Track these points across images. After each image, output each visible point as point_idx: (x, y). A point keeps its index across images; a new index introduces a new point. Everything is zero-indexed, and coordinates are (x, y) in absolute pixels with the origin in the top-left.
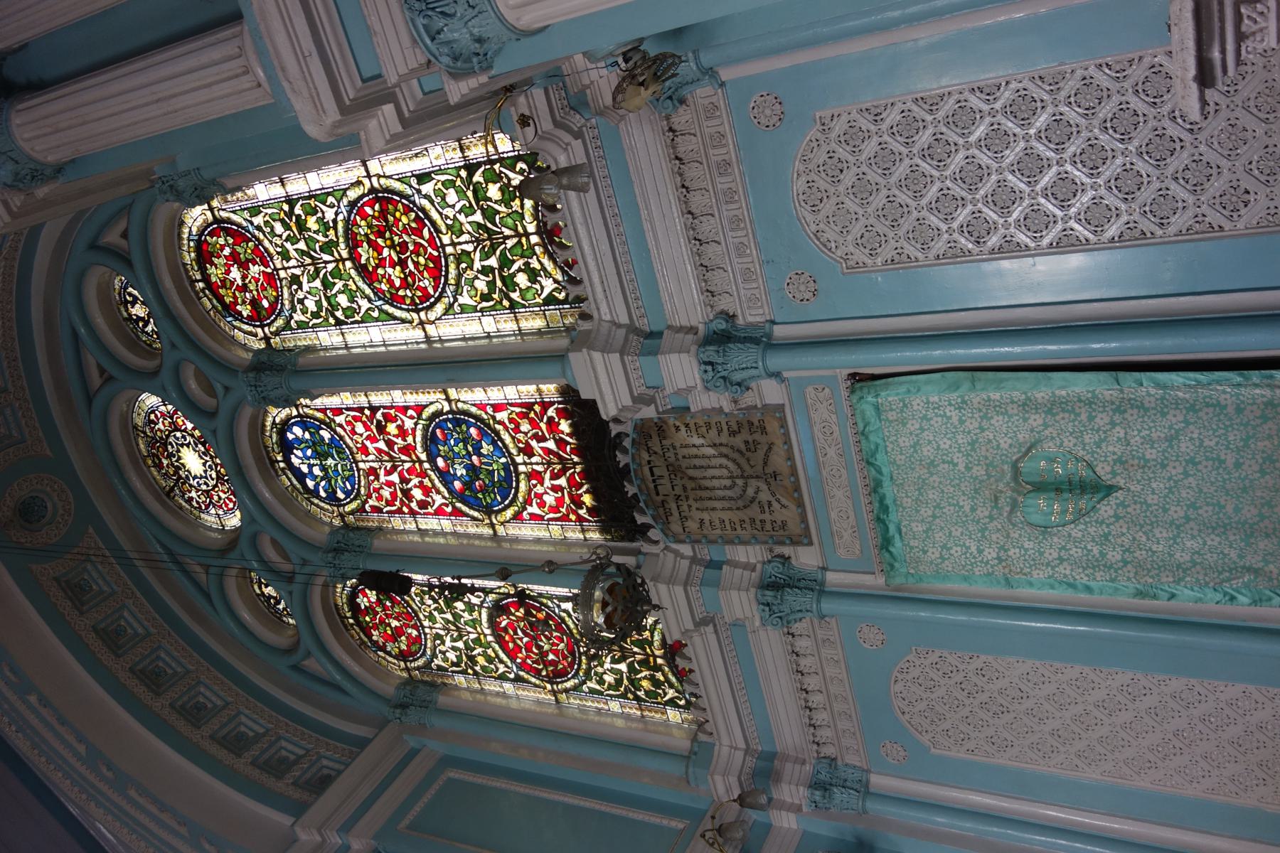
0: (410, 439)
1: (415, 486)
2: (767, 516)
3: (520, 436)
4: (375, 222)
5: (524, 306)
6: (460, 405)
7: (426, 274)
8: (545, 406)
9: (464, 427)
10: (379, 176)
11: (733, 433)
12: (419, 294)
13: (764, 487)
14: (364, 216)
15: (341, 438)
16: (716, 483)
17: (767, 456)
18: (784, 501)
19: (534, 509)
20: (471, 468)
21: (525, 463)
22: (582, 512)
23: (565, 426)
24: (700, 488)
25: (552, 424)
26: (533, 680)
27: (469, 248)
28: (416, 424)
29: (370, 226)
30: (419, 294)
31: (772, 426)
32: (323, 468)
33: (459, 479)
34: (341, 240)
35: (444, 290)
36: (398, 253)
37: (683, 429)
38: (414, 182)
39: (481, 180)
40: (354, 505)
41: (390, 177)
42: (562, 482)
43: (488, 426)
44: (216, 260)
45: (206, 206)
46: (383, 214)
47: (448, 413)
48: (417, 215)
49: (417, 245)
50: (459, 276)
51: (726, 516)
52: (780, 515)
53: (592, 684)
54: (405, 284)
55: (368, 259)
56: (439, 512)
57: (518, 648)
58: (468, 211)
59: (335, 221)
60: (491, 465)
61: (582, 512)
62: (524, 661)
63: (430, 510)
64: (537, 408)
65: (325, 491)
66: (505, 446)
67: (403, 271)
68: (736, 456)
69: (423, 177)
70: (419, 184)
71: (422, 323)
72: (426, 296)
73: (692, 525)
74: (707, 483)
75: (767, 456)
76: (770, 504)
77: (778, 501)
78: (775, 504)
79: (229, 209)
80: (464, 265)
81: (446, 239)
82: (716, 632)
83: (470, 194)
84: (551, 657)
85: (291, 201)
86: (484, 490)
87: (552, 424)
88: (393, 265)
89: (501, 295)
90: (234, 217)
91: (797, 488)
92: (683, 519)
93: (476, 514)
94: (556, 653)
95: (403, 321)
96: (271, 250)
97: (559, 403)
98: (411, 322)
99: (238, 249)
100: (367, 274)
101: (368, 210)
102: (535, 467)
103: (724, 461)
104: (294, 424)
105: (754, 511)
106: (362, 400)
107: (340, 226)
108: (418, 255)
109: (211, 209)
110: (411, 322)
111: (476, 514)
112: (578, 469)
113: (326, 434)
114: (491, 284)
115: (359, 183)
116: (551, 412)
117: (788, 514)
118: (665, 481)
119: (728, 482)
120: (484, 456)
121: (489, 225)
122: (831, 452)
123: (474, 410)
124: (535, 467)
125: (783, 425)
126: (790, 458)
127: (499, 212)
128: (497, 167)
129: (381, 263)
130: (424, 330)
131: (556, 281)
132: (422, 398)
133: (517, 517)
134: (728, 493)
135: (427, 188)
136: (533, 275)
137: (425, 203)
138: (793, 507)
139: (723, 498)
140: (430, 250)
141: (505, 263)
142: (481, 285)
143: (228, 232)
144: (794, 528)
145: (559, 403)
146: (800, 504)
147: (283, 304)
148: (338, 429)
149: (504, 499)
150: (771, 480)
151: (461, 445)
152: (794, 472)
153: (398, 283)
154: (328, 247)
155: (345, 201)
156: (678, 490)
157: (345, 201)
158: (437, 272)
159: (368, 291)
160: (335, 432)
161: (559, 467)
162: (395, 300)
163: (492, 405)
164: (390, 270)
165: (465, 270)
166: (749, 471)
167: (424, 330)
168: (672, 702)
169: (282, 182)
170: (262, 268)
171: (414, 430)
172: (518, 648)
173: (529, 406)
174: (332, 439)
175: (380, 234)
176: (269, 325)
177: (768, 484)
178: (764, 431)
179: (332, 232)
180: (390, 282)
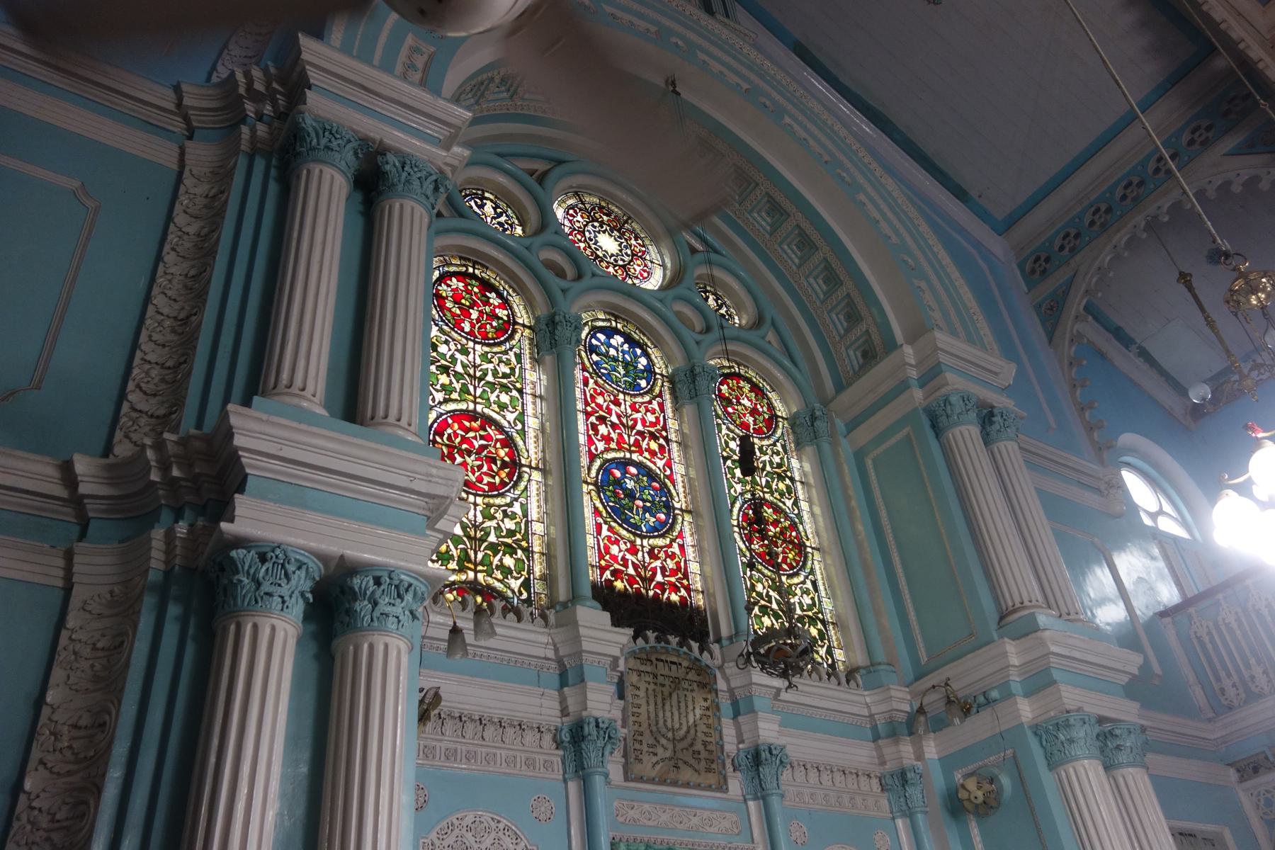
2: (645, 748)
8: (688, 589)
11: (705, 744)
13: (668, 754)
16: (668, 714)
17: (691, 766)
18: (658, 767)
19: (605, 532)
20: (631, 495)
22: (607, 574)
23: (674, 598)
24: (664, 699)
31: (712, 779)
32: (615, 359)
37: (706, 704)
40: (587, 364)
42: (631, 571)
46: (791, 542)
51: (643, 710)
52: (648, 760)
56: (591, 442)
57: (467, 430)
61: (607, 574)
63: (591, 432)
66: (654, 537)
68: (689, 740)
69: (814, 583)
73: (634, 678)
74: (667, 707)
75: (691, 766)
76: (655, 754)
77: (657, 763)
78: (654, 759)
82: (546, 658)
84: (459, 460)
86: (615, 494)
91: (663, 782)
92: (640, 673)
103: (685, 728)
105: (647, 739)
116: (683, 592)
117: (647, 766)
118: (666, 672)
119: (669, 724)
122: (695, 821)
125: (709, 788)
126: (687, 785)
133: (597, 512)
134: (661, 722)
135: (809, 585)
137: (801, 578)
138: (653, 774)
139: (657, 715)
143: (771, 418)
144: (637, 769)
146: (651, 781)
150: (672, 763)
152: (674, 783)
154: (768, 485)
156: (661, 679)
166: (680, 746)
172: (462, 427)
174: (638, 387)
175: (782, 532)
177: (670, 759)
178: (708, 770)
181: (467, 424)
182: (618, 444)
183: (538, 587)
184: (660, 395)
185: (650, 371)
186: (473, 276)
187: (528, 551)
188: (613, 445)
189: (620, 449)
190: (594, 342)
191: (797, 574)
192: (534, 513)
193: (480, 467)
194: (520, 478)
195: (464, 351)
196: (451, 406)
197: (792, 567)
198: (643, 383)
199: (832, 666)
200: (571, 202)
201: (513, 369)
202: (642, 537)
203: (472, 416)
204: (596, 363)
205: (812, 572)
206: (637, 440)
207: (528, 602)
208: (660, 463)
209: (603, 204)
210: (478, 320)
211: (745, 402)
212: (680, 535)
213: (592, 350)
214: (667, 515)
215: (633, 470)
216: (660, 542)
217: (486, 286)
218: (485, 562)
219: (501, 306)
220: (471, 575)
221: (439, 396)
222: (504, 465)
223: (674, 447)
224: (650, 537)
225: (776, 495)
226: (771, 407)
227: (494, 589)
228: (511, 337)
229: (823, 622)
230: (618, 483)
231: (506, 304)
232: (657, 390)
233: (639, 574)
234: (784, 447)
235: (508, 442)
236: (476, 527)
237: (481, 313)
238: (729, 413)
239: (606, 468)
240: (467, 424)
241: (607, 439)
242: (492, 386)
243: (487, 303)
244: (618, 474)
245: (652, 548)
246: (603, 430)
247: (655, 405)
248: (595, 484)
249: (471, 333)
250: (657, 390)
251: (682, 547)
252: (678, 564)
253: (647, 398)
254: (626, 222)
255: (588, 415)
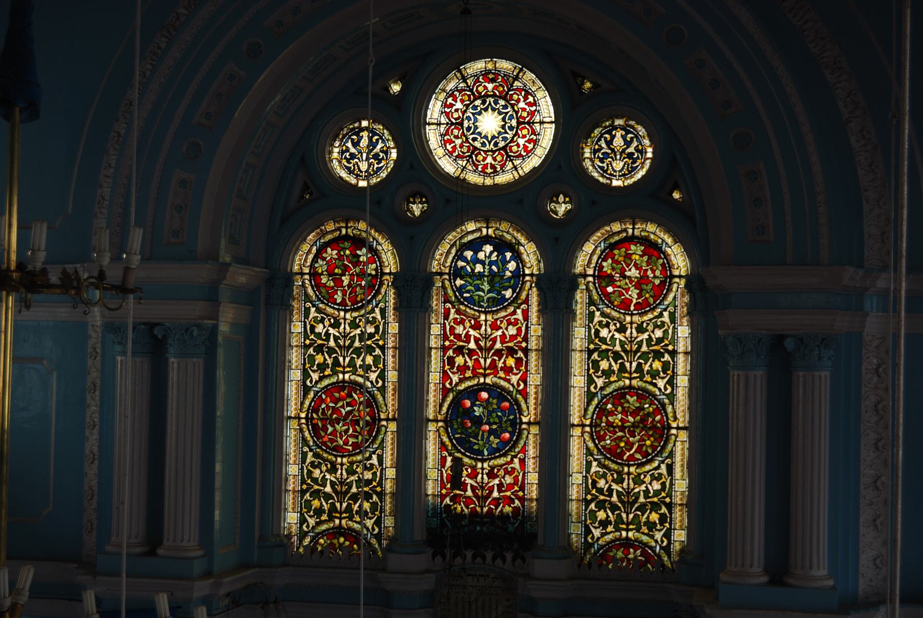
0: (502, 374)
1: (466, 362)
3: (502, 472)
4: (650, 419)
5: (586, 510)
6: (525, 432)
7: (614, 443)
8: (522, 500)
9: (510, 429)
10: (677, 437)
12: (602, 433)
14: (656, 412)
15: (505, 308)
20: (478, 421)
21: (483, 469)
22: (447, 500)
25: (510, 501)
26: (307, 403)
27: (625, 485)
28: (513, 385)
29: (649, 414)
30: (602, 433)
32: (481, 276)
33: (472, 407)
34: (644, 385)
35: (602, 454)
36: (629, 427)
38: (668, 461)
39: (662, 511)
41: (674, 445)
43: (510, 450)
44: (645, 258)
45: (683, 274)
46: (654, 427)
47: (521, 419)
48: (650, 454)
49: (632, 445)
50: (609, 469)
53: (310, 457)
54: (609, 424)
55: (628, 402)
56: (445, 376)
57: (336, 401)
58: (647, 492)
59: (655, 385)
60: (482, 440)
61: (447, 500)
62: (323, 401)
63: (447, 367)
64: (521, 494)
65: (462, 267)
66: (496, 458)
67: (617, 426)
69: (670, 469)
70: (667, 464)
71: (583, 426)
72: (602, 438)
79: (677, 295)
80: (615, 476)
81: (632, 469)
83: (655, 499)
84: (330, 429)
85: (673, 353)
86: (463, 424)
87: (510, 501)
88: (622, 420)
89: (595, 497)
90: (671, 296)
93: (445, 409)
94: (334, 433)
95: (586, 410)
96: (646, 318)
97: (524, 511)
98: (584, 416)
99: (650, 286)
100: (619, 396)
101: (658, 418)
102: (480, 476)
104: (518, 265)
106: (533, 344)
107: (650, 387)
108: (626, 443)
109: (680, 277)
110: (584, 416)
111: (445, 409)
112: (478, 509)
113: (508, 294)
114: (600, 491)
115: (675, 419)
120: (489, 437)
121: (636, 505)
123: (522, 442)
124: (480, 476)
127: (643, 515)
128: (667, 525)
129: (625, 412)
130: (578, 425)
131: (598, 539)
132: (532, 401)
133: (443, 446)
136: (604, 524)
137: (656, 464)
140: (628, 454)
141: (614, 508)
142: (602, 483)
143: (663, 283)
145: (524, 511)
147: (608, 307)
148: (512, 309)
149: (456, 439)
151: (497, 420)
153: (610, 418)
155: (666, 401)
157: (666, 401)
158: (614, 453)
159: (608, 390)
160: (509, 305)
161: (480, 494)
162: (601, 411)
163: (524, 459)
164: (620, 416)
165: (612, 475)
167: (578, 425)
168: (303, 521)
169: (686, 353)
170: (634, 301)
171: (508, 381)
172: (336, 401)
173: (522, 488)
174: (504, 299)
175: (643, 420)
176: (594, 283)
179: (649, 379)
180: (611, 413)
181: (337, 395)
182: (474, 371)
183: (389, 522)
184: (526, 301)
185: (518, 274)
186: (347, 237)
187: (381, 495)
188: (469, 374)
189: (475, 375)
190: (461, 264)
191: (652, 460)
192: (388, 460)
193: (347, 431)
194: (378, 432)
195: (336, 325)
196: (326, 382)
197: (645, 454)
198: (508, 294)
199: (667, 549)
200: (451, 86)
201: (377, 328)
202: (483, 461)
203: (340, 386)
204: (461, 289)
205: (671, 455)
206: (493, 361)
207: (378, 537)
208: (514, 379)
209: (490, 66)
210: (349, 285)
211: (633, 273)
212: (524, 450)
213: (457, 273)
214: (512, 434)
215: (484, 395)
216: (501, 461)
217: (358, 242)
218: (349, 509)
219: (371, 261)
220: (337, 521)
221: (315, 376)
222: (367, 423)
223: (533, 356)
224: (490, 459)
225: (648, 378)
226: (667, 266)
227: (353, 530)
228: (378, 292)
229: (670, 506)
230: (469, 412)
231: (375, 253)
232: (523, 296)
233: (476, 495)
234: (672, 317)
235: (371, 403)
236: (342, 483)
237: (352, 276)
238: (607, 295)
239: (456, 404)
240: (337, 395)
241: (463, 369)
242: (358, 351)
243: (356, 263)
244: (468, 403)
245: (492, 468)
246: (459, 360)
247: (519, 315)
248: (445, 421)
249: (343, 303)
250: (523, 296)
251: (522, 462)
252: (516, 478)
253: (512, 309)
254: (516, 78)
255: (444, 349)
